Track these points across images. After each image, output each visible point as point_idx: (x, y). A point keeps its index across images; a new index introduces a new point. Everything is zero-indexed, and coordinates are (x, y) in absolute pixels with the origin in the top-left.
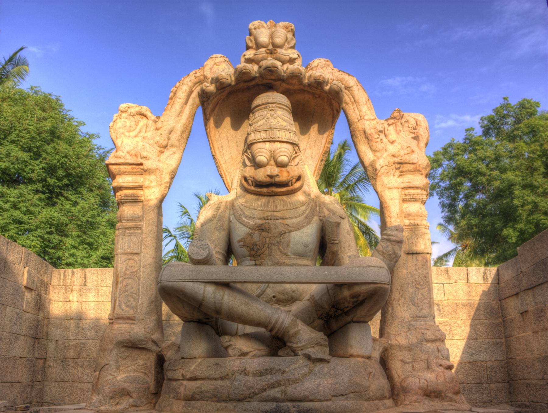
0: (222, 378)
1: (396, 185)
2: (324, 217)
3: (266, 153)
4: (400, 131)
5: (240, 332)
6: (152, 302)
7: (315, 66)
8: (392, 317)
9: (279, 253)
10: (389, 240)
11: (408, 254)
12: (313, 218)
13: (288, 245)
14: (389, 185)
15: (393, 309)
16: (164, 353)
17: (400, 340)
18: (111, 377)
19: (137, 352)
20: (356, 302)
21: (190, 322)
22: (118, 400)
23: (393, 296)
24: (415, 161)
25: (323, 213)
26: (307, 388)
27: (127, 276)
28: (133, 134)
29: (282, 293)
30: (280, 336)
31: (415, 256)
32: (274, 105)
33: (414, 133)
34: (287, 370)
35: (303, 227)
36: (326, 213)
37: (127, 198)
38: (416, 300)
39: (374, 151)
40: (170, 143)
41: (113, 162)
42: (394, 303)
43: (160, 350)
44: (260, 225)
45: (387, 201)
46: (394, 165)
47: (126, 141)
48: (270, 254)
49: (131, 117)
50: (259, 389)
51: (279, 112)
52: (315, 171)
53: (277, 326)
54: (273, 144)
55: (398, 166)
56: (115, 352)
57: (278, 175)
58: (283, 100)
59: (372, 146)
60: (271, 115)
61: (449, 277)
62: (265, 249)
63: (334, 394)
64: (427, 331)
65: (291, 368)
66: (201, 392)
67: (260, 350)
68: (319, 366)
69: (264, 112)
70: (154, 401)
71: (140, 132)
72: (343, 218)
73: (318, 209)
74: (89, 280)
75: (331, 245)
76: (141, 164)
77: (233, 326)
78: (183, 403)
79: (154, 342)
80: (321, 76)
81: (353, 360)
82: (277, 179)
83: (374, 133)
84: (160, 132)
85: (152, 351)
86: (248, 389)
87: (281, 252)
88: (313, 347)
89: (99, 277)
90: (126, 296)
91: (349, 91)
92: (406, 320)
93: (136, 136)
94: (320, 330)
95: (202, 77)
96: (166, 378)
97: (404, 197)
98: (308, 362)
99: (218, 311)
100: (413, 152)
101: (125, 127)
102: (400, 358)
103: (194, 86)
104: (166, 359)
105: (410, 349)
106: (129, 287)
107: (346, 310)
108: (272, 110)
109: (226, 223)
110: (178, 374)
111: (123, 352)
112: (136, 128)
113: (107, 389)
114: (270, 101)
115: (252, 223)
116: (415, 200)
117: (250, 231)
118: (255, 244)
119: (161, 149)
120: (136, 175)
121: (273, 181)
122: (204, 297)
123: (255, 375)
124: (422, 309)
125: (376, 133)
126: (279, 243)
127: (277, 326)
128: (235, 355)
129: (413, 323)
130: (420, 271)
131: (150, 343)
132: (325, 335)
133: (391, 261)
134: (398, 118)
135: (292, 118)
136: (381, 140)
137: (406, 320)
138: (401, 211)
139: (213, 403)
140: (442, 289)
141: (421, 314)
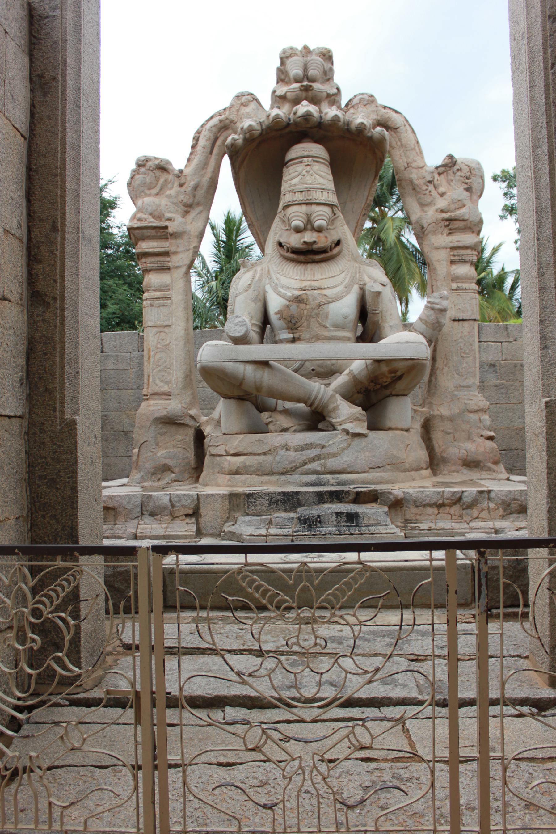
0: (265, 454)
1: (444, 244)
2: (365, 284)
3: (302, 217)
4: (452, 181)
5: (280, 408)
6: (187, 376)
7: (357, 104)
8: (436, 387)
9: (318, 325)
10: (433, 309)
11: (454, 320)
12: (352, 287)
13: (327, 317)
14: (436, 245)
15: (436, 379)
16: (202, 428)
17: (442, 411)
18: (151, 454)
19: (174, 428)
20: (394, 377)
21: (230, 398)
22: (159, 476)
23: (437, 366)
24: (466, 218)
25: (364, 280)
26: (346, 461)
27: (159, 350)
28: (154, 191)
29: (321, 366)
30: (320, 411)
31: (461, 322)
32: (310, 159)
33: (467, 183)
34: (326, 445)
35: (342, 297)
36: (367, 279)
37: (152, 265)
38: (461, 370)
39: (422, 205)
40: (196, 201)
41: (135, 226)
42: (438, 372)
43: (198, 425)
44: (297, 297)
45: (435, 263)
46: (443, 223)
47: (147, 200)
48: (308, 327)
49: (150, 172)
50: (300, 463)
51: (316, 167)
52: (356, 228)
53: (317, 402)
54: (309, 206)
55: (447, 223)
56: (153, 428)
57: (315, 242)
58: (320, 153)
59: (420, 198)
60: (308, 172)
61: (508, 335)
62: (303, 321)
63: (371, 466)
64: (470, 402)
65: (331, 442)
66: (245, 467)
67: (300, 425)
68: (357, 441)
69: (300, 168)
70: (195, 475)
71: (161, 189)
72: (384, 286)
73: (358, 276)
74: (106, 346)
75: (371, 315)
76: (166, 227)
77: (273, 401)
78: (228, 477)
79: (192, 417)
80: (362, 123)
81: (390, 433)
82: (315, 246)
83: (422, 184)
84: (184, 188)
85: (190, 427)
86: (290, 463)
87: (320, 324)
88: (352, 422)
89: (117, 342)
90: (160, 371)
91: (395, 132)
92: (449, 390)
93: (157, 194)
94: (358, 405)
95: (227, 121)
96: (208, 453)
97: (452, 258)
98: (346, 437)
99: (259, 389)
100: (464, 206)
101: (145, 183)
102: (442, 429)
103: (219, 131)
104: (205, 434)
105: (451, 419)
106: (163, 360)
107: (384, 384)
108: (308, 165)
109: (262, 293)
110: (221, 450)
111: (161, 428)
112: (157, 184)
113: (149, 465)
114: (306, 154)
115: (289, 294)
116: (464, 262)
117: (287, 303)
118: (292, 317)
119: (186, 209)
120: (161, 239)
121: (310, 248)
122: (244, 376)
123: (296, 450)
124: (466, 379)
125: (425, 184)
126: (318, 315)
127: (317, 402)
128: (276, 431)
129: (456, 393)
130: (466, 339)
131: (188, 418)
132: (363, 409)
133: (434, 330)
134: (450, 165)
135: (330, 172)
136: (430, 192)
137: (449, 390)
138: (449, 273)
139: (257, 477)
140: (500, 348)
141: (464, 384)
